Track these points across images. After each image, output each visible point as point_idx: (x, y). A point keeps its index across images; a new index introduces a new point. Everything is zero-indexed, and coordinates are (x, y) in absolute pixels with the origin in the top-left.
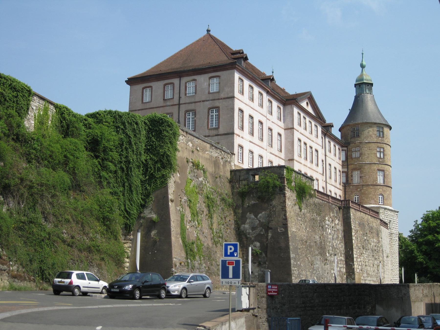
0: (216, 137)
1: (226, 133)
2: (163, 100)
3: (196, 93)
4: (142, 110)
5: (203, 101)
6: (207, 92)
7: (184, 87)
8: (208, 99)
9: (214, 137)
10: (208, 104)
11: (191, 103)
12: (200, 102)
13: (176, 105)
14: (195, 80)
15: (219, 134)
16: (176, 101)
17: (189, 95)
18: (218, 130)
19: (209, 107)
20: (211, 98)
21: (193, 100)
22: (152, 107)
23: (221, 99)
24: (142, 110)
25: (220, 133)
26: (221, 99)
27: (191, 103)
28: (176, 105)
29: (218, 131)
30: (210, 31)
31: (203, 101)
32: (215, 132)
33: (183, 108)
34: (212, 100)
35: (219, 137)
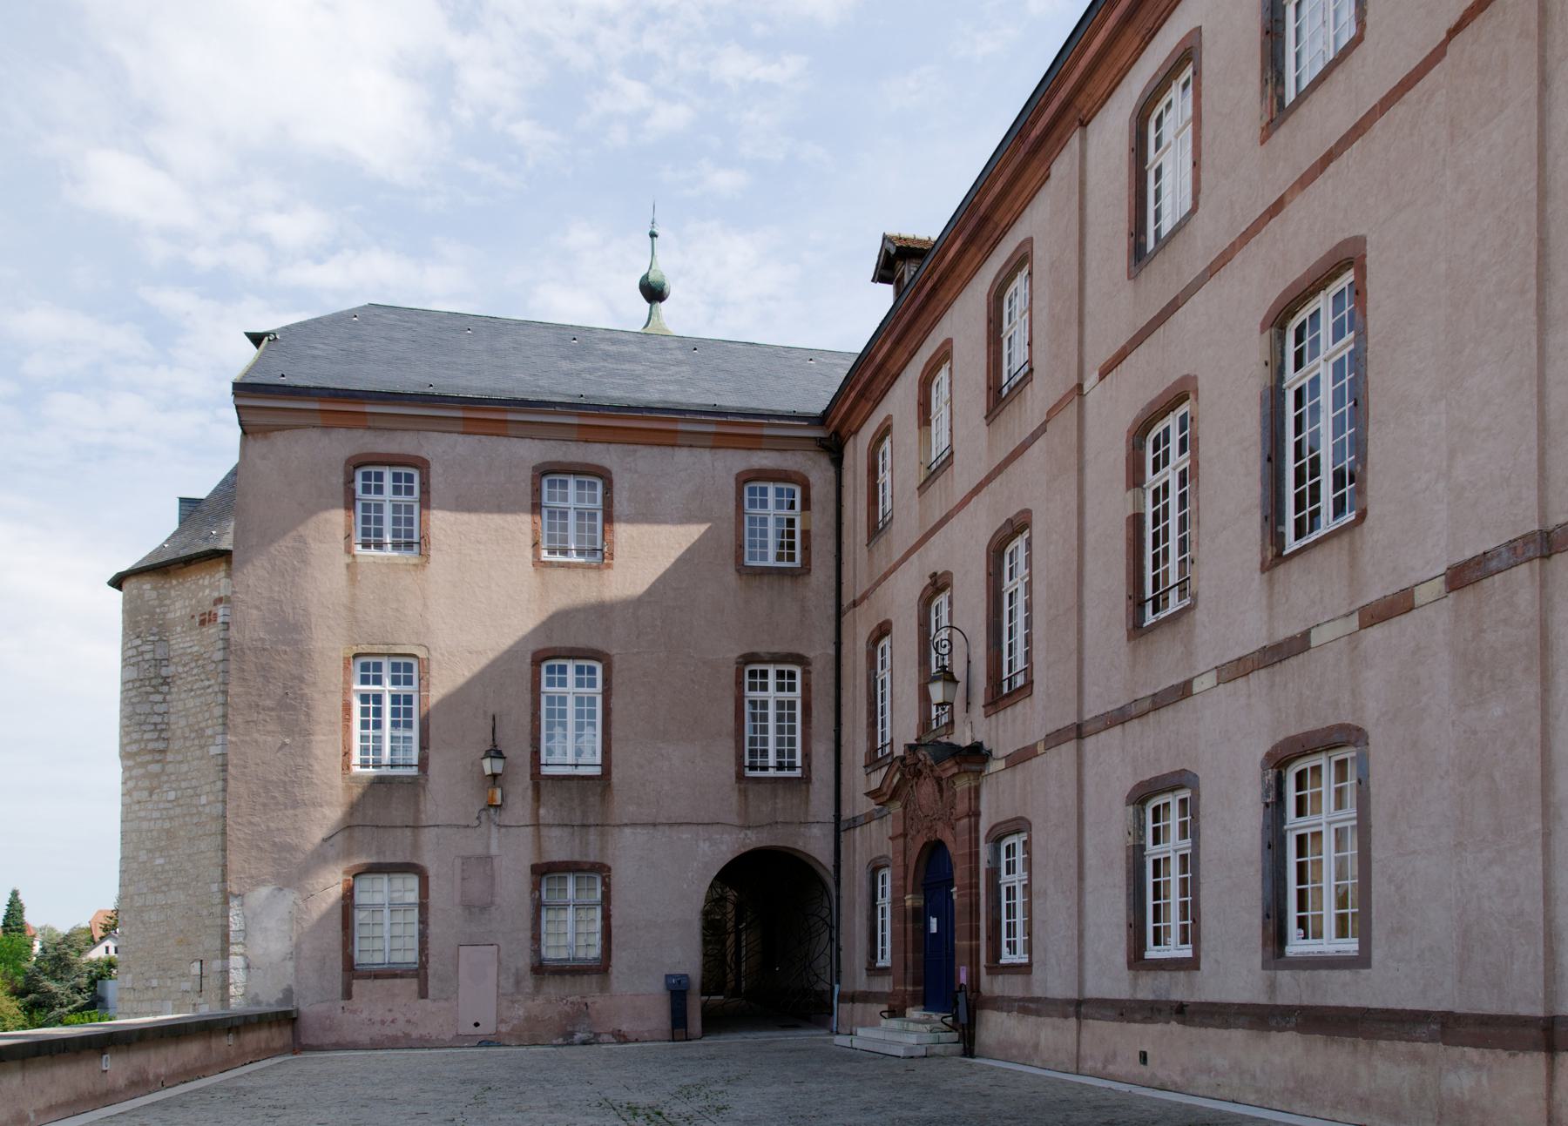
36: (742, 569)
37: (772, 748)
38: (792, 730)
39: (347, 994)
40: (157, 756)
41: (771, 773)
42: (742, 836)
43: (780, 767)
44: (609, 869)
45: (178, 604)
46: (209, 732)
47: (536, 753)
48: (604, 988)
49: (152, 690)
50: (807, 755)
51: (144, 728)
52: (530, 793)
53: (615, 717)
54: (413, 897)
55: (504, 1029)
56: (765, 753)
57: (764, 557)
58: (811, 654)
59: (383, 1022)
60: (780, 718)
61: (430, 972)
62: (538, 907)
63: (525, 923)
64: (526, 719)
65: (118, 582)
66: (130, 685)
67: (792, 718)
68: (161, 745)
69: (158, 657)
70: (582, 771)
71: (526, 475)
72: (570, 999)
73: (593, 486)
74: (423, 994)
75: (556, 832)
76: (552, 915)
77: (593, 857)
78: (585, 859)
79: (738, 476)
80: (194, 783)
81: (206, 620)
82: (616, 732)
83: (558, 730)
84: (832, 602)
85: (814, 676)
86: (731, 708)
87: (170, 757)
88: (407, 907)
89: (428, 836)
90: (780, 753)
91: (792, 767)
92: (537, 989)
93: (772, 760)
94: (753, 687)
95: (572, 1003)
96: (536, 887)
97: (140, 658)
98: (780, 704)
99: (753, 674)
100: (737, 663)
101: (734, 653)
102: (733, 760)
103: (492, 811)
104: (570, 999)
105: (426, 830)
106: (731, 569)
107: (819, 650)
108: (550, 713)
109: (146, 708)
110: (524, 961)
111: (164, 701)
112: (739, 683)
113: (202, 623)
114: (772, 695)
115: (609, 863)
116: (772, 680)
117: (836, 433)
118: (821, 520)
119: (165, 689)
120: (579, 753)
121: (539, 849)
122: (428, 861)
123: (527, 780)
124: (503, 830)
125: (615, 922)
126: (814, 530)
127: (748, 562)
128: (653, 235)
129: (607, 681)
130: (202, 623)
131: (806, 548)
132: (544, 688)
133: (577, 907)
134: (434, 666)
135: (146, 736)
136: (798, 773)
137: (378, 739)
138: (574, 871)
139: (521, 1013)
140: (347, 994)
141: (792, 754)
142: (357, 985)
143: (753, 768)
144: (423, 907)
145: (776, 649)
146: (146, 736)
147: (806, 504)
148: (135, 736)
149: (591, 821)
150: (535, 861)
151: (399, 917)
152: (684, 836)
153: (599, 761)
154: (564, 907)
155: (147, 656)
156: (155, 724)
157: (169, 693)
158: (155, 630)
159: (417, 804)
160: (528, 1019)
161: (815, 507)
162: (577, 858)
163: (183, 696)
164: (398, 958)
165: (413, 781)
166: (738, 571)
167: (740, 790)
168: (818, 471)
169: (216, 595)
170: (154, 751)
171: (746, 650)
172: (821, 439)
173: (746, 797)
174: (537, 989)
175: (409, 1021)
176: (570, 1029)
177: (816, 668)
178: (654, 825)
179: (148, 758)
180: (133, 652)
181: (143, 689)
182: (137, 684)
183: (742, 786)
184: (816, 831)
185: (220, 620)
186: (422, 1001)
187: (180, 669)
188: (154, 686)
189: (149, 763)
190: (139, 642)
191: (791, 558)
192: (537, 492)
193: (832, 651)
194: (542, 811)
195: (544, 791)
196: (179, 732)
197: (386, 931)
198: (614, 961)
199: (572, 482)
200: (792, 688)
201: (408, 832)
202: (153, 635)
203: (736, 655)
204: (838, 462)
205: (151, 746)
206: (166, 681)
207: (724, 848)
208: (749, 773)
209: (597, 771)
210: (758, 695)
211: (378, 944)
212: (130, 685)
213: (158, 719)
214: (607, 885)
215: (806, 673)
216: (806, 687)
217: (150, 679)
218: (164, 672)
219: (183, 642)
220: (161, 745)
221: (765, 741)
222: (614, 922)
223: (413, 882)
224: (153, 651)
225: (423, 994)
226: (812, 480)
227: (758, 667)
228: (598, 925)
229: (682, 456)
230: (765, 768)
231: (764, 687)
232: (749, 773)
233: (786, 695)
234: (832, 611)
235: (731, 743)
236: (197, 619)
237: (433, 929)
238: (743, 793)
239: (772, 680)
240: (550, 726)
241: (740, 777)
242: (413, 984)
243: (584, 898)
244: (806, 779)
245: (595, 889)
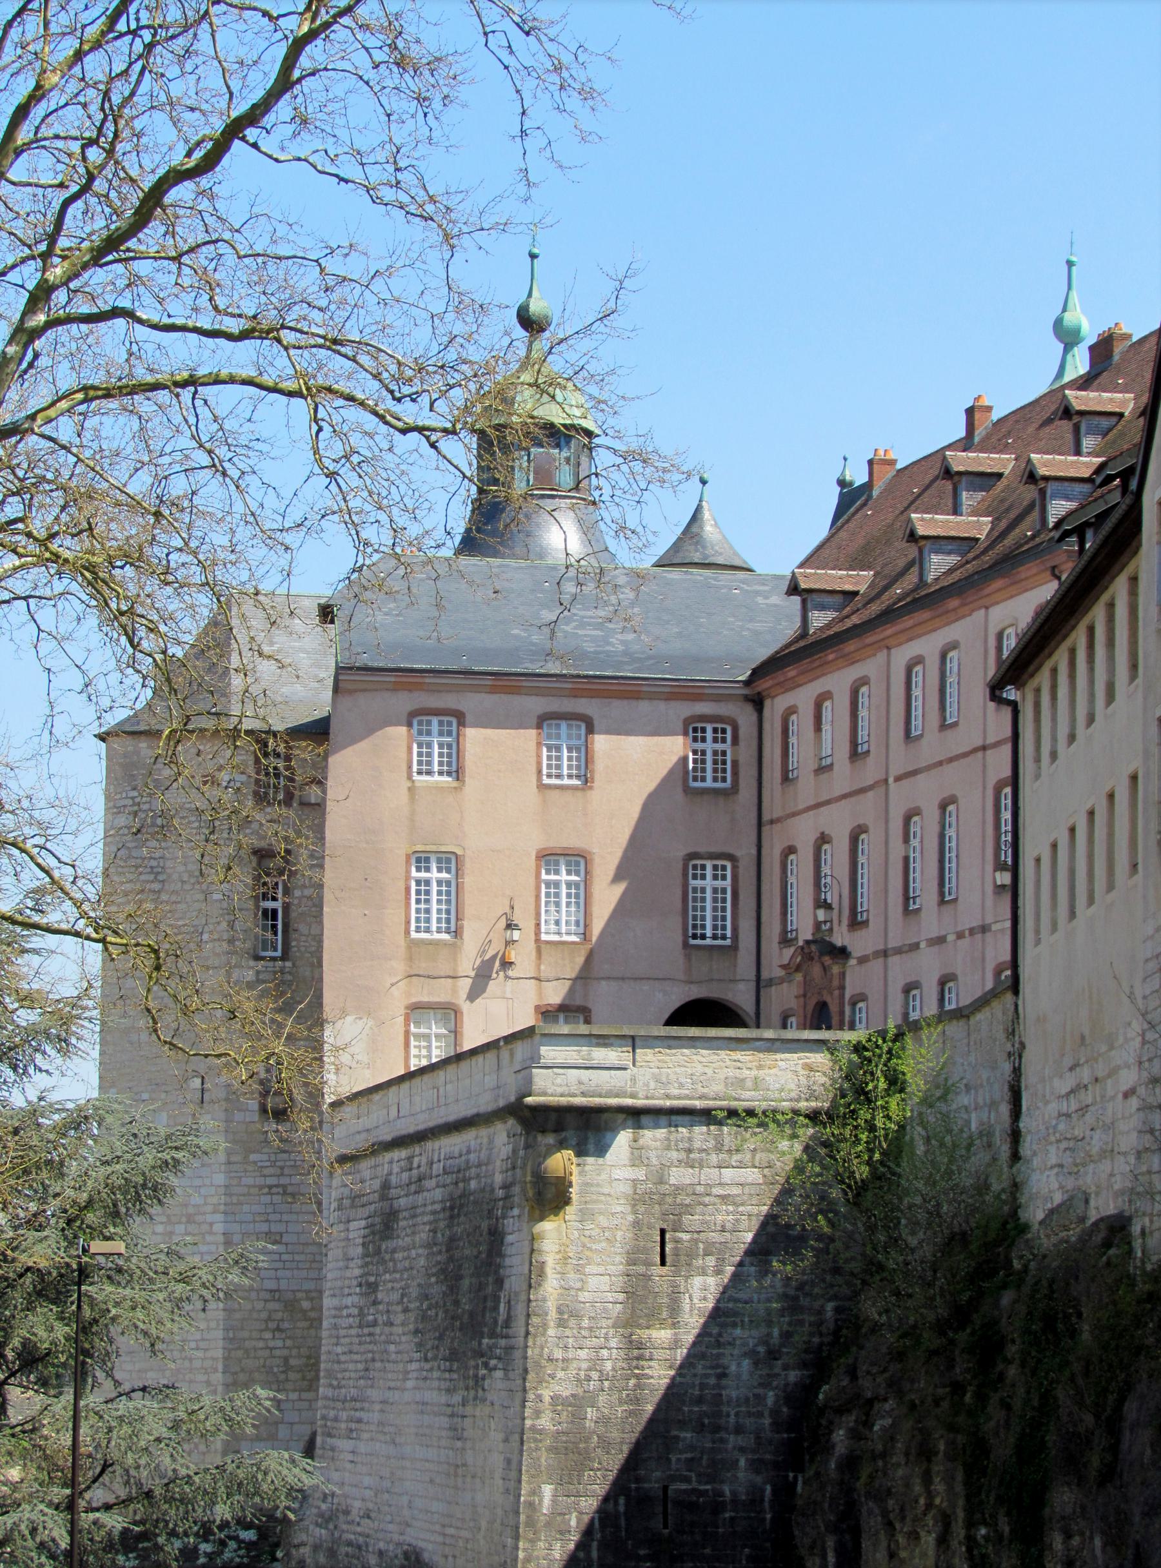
37: (709, 923)
38: (724, 909)
41: (708, 942)
43: (715, 937)
52: (534, 953)
56: (703, 927)
57: (703, 779)
58: (738, 854)
65: (102, 737)
67: (724, 900)
68: (156, 886)
73: (579, 727)
84: (754, 814)
85: (741, 871)
87: (164, 897)
90: (715, 927)
91: (724, 937)
93: (709, 932)
94: (695, 877)
98: (715, 890)
99: (695, 867)
101: (681, 853)
102: (680, 931)
107: (745, 851)
114: (709, 883)
115: (590, 1005)
116: (709, 872)
118: (746, 753)
121: (540, 994)
123: (532, 945)
126: (742, 760)
131: (735, 774)
134: (467, 860)
136: (728, 942)
137: (428, 911)
141: (724, 928)
143: (695, 937)
145: (713, 849)
147: (735, 740)
159: (455, 960)
161: (742, 743)
168: (745, 717)
177: (742, 864)
178: (623, 979)
184: (741, 986)
190: (135, 794)
191: (724, 780)
193: (754, 851)
196: (175, 876)
199: (564, 725)
200: (724, 878)
208: (693, 942)
210: (698, 883)
213: (154, 863)
215: (735, 868)
220: (156, 886)
221: (703, 918)
227: (699, 862)
230: (703, 937)
231: (703, 877)
232: (693, 942)
233: (719, 883)
234: (754, 821)
235: (679, 919)
238: (688, 957)
239: (709, 872)
241: (686, 945)
244: (734, 947)
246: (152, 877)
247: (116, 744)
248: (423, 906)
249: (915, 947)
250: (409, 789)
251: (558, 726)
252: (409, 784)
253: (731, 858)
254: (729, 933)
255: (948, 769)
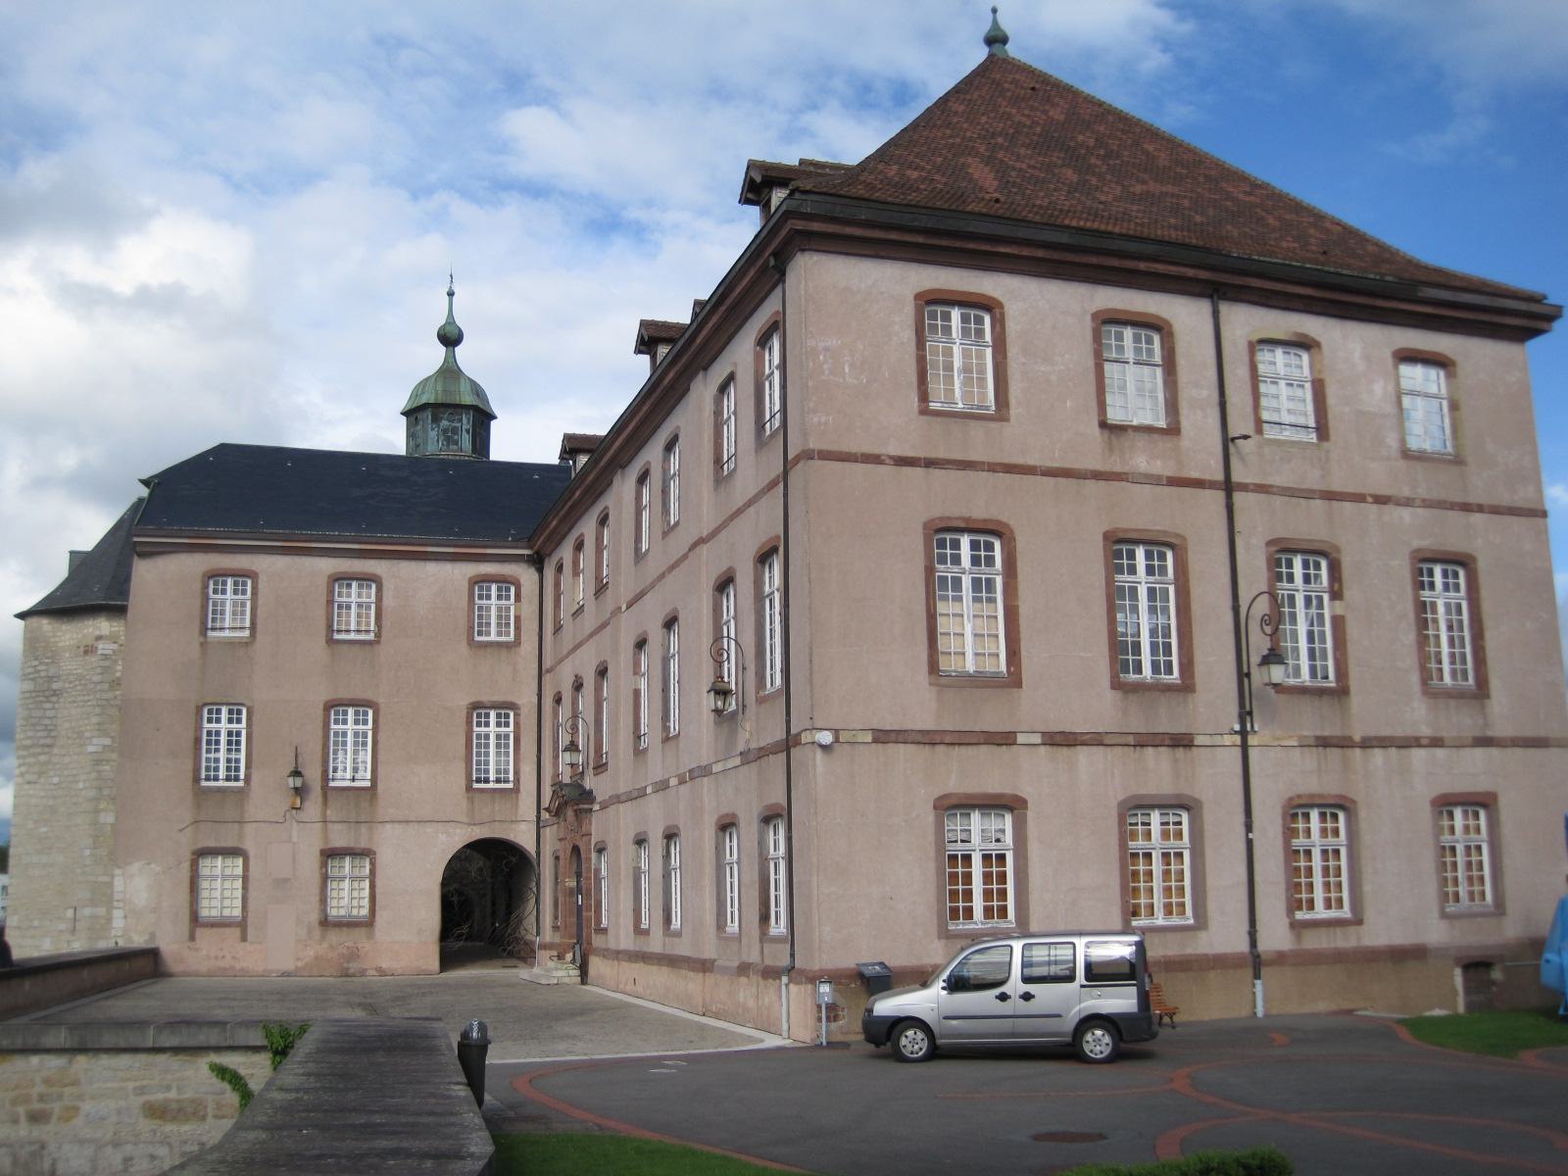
0: (1479, 752)
1: (1529, 732)
2: (1096, 424)
3: (1322, 429)
4: (930, 463)
5: (1381, 500)
6: (1392, 441)
7: (1243, 372)
8: (1406, 492)
9: (1468, 752)
10: (1414, 529)
11: (1308, 494)
12: (1359, 498)
13: (1198, 484)
14: (1304, 344)
15: (1489, 733)
16: (1201, 452)
17: (1288, 434)
18: (1483, 707)
19: (1416, 543)
20: (1422, 492)
21: (1313, 480)
22: (1019, 460)
23: (1480, 509)
24: (930, 463)
25: (1500, 729)
26: (1480, 509)
27: (1308, 494)
28: (1198, 484)
29: (1485, 716)
30: (1004, 40)
31: (1381, 500)
32: (1462, 721)
33: (1259, 521)
34: (1427, 504)
35: (1494, 751)
36: (471, 641)
37: (492, 768)
38: (507, 754)
39: (192, 938)
40: (46, 750)
41: (491, 785)
42: (469, 830)
43: (498, 781)
44: (375, 853)
45: (67, 637)
46: (87, 734)
47: (325, 772)
48: (370, 936)
49: (45, 700)
50: (517, 773)
51: (38, 728)
53: (380, 746)
54: (239, 871)
55: (299, 964)
57: (488, 634)
58: (519, 702)
59: (216, 958)
60: (498, 746)
61: (249, 923)
62: (325, 878)
63: (316, 890)
64: (319, 748)
66: (28, 695)
67: (507, 746)
69: (50, 675)
70: (357, 784)
71: (322, 582)
72: (346, 944)
74: (244, 938)
75: (337, 827)
76: (335, 885)
77: (363, 844)
78: (358, 846)
79: (470, 579)
80: (75, 772)
81: (89, 650)
82: (381, 757)
83: (340, 754)
86: (463, 741)
87: (55, 751)
88: (234, 877)
89: (249, 829)
91: (506, 781)
92: (323, 938)
94: (479, 724)
95: (348, 947)
96: (324, 865)
97: (37, 675)
98: (498, 737)
99: (479, 716)
100: (468, 708)
101: (464, 701)
102: (463, 777)
103: (294, 811)
104: (346, 944)
105: (249, 824)
106: (464, 643)
107: (527, 699)
108: (336, 743)
109: (39, 713)
110: (314, 917)
111: (54, 708)
112: (469, 723)
113: (86, 652)
114: (492, 729)
115: (375, 849)
117: (537, 553)
118: (529, 609)
119: (54, 699)
120: (355, 770)
121: (326, 838)
122: (249, 846)
124: (301, 825)
125: (378, 890)
127: (478, 638)
128: (451, 294)
129: (375, 721)
130: (86, 652)
131: (518, 628)
132: (333, 726)
133: (353, 879)
135: (39, 734)
136: (510, 785)
138: (350, 855)
139: (312, 953)
140: (192, 938)
142: (199, 932)
143: (478, 781)
144: (245, 878)
146: (39, 734)
148: (30, 734)
149: (363, 819)
150: (322, 847)
151: (227, 884)
152: (429, 830)
153: (369, 777)
154: (342, 879)
155: (43, 674)
156: (46, 725)
157: (58, 702)
158: (49, 654)
160: (316, 958)
162: (352, 845)
163: (67, 705)
164: (226, 912)
165: (240, 790)
166: (469, 644)
167: (468, 798)
169: (97, 633)
170: (43, 746)
171: (473, 699)
172: (528, 555)
173: (473, 803)
174: (323, 938)
175: (234, 958)
176: (345, 965)
177: (524, 712)
178: (407, 822)
179: (39, 750)
180: (31, 670)
181: (38, 699)
182: (34, 694)
183: (470, 795)
184: (523, 826)
185: (100, 652)
186: (243, 944)
187: (67, 685)
188: (46, 697)
189: (39, 754)
190: (37, 663)
192: (331, 592)
194: (329, 812)
195: (330, 798)
197: (217, 894)
198: (377, 918)
200: (507, 725)
201: (236, 826)
202: (47, 658)
203: (467, 703)
204: (540, 571)
205: (42, 741)
206: (55, 693)
207: (457, 838)
208: (476, 786)
209: (368, 784)
210: (483, 729)
211: (215, 903)
212: (28, 695)
213: (48, 722)
214: (373, 864)
215: (516, 715)
216: (517, 724)
217: (44, 691)
218: (55, 686)
219: (70, 665)
220: (48, 741)
221: (487, 763)
222: (378, 890)
223: (240, 861)
224: (47, 670)
225: (244, 938)
226: (522, 581)
227: (483, 711)
228: (366, 893)
229: (432, 567)
230: (487, 781)
231: (487, 724)
232: (476, 786)
234: (536, 672)
235: (462, 766)
236: (82, 649)
237: (252, 894)
238: (471, 800)
240: (336, 752)
241: (469, 788)
242: (237, 932)
243: (356, 872)
244: (516, 790)
245: (364, 867)
246: (45, 734)
247: (34, 621)
248: (212, 756)
249: (641, 794)
250: (202, 644)
251: (349, 586)
252: (202, 639)
253: (512, 706)
254: (511, 778)
255: (670, 578)
